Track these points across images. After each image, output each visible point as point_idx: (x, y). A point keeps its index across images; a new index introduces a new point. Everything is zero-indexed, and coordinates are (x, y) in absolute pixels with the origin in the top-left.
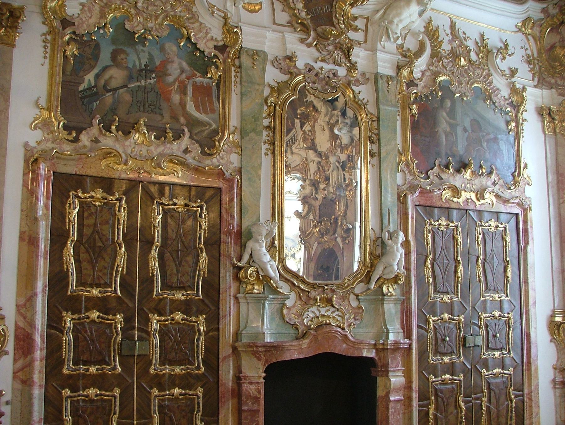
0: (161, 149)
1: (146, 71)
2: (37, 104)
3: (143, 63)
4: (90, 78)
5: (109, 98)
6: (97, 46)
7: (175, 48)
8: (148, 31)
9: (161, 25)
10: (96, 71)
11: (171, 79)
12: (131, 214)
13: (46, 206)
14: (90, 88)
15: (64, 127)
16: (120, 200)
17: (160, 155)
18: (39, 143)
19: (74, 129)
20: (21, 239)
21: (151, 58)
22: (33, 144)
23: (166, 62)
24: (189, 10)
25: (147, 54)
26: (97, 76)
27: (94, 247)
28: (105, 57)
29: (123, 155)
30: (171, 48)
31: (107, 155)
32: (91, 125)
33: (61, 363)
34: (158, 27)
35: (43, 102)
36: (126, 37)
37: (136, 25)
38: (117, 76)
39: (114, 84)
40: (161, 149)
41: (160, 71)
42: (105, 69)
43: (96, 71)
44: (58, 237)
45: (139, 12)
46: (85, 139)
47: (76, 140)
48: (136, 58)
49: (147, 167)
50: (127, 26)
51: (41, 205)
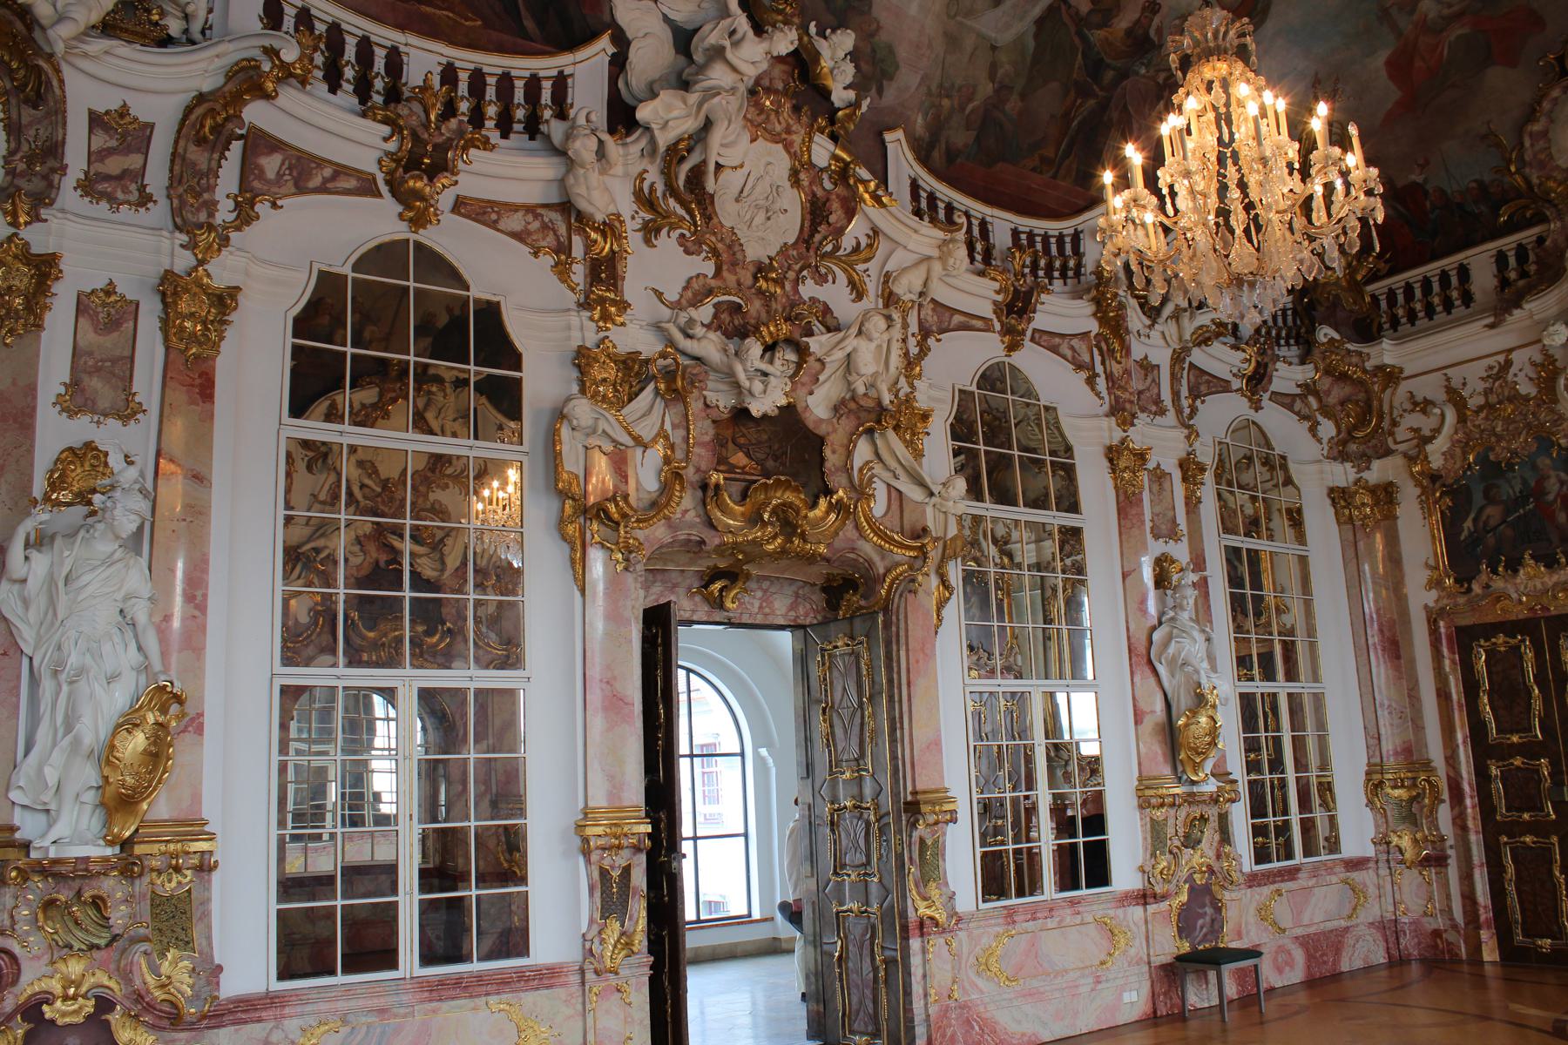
0: (1555, 578)
1: (1521, 500)
2: (1427, 565)
3: (1517, 489)
4: (1468, 524)
5: (1490, 539)
6: (1467, 491)
7: (1548, 461)
8: (1515, 453)
9: (1526, 441)
10: (1472, 516)
11: (1551, 497)
12: (1539, 655)
13: (1453, 662)
14: (1471, 534)
15: (1456, 581)
16: (1523, 641)
17: (1556, 584)
18: (1437, 601)
19: (1464, 579)
20: (1439, 695)
21: (1524, 482)
22: (1431, 604)
23: (1542, 480)
24: (1552, 411)
25: (1519, 480)
26: (1475, 520)
27: (1509, 694)
28: (1478, 498)
29: (1514, 596)
30: (1544, 462)
31: (1498, 599)
32: (1479, 572)
33: (1493, 810)
34: (1522, 442)
35: (1432, 562)
36: (1492, 470)
37: (1500, 453)
38: (1493, 513)
39: (1493, 522)
40: (1555, 578)
41: (1539, 491)
42: (1481, 509)
43: (1472, 516)
44: (1471, 688)
45: (1499, 438)
46: (1476, 588)
47: (1469, 590)
48: (1510, 488)
49: (1545, 601)
50: (1492, 457)
51: (1447, 662)
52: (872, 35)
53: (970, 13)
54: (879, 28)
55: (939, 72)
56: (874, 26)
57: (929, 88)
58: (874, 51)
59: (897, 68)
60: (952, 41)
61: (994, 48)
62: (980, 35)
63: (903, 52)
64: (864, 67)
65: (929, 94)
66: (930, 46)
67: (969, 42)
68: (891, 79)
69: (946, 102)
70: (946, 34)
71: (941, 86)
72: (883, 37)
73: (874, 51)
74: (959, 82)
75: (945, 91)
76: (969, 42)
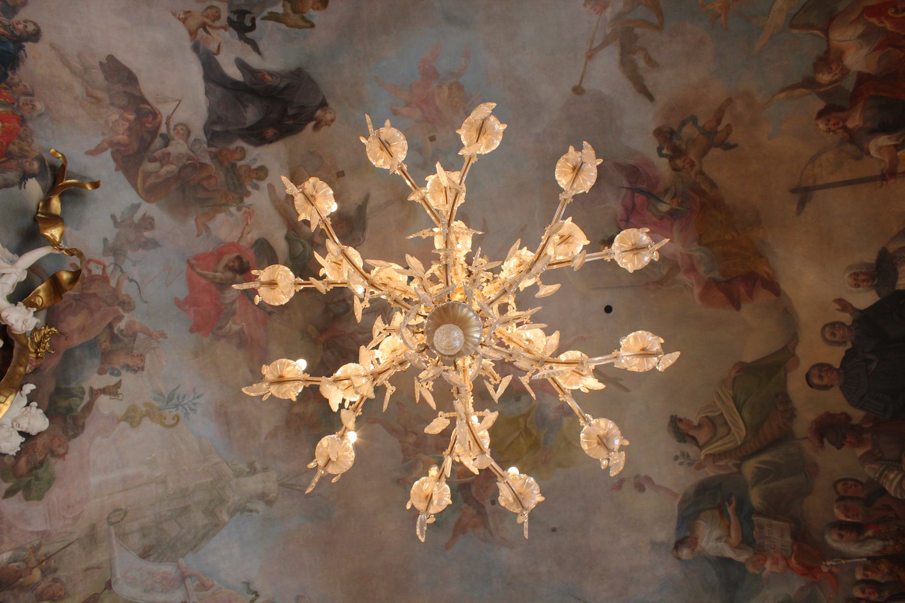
52: (53, 453)
53: (123, 536)
54: (62, 456)
55: (59, 546)
56: (61, 451)
57: (40, 545)
58: (41, 463)
59: (40, 498)
60: (92, 539)
61: (109, 585)
62: (110, 561)
63: (55, 494)
64: (23, 462)
65: (35, 549)
66: (76, 519)
67: (100, 557)
68: (27, 498)
69: (37, 574)
70: (93, 527)
71: (48, 557)
72: (57, 466)
73: (41, 463)
74: (61, 574)
75: (47, 565)
76: (100, 557)
